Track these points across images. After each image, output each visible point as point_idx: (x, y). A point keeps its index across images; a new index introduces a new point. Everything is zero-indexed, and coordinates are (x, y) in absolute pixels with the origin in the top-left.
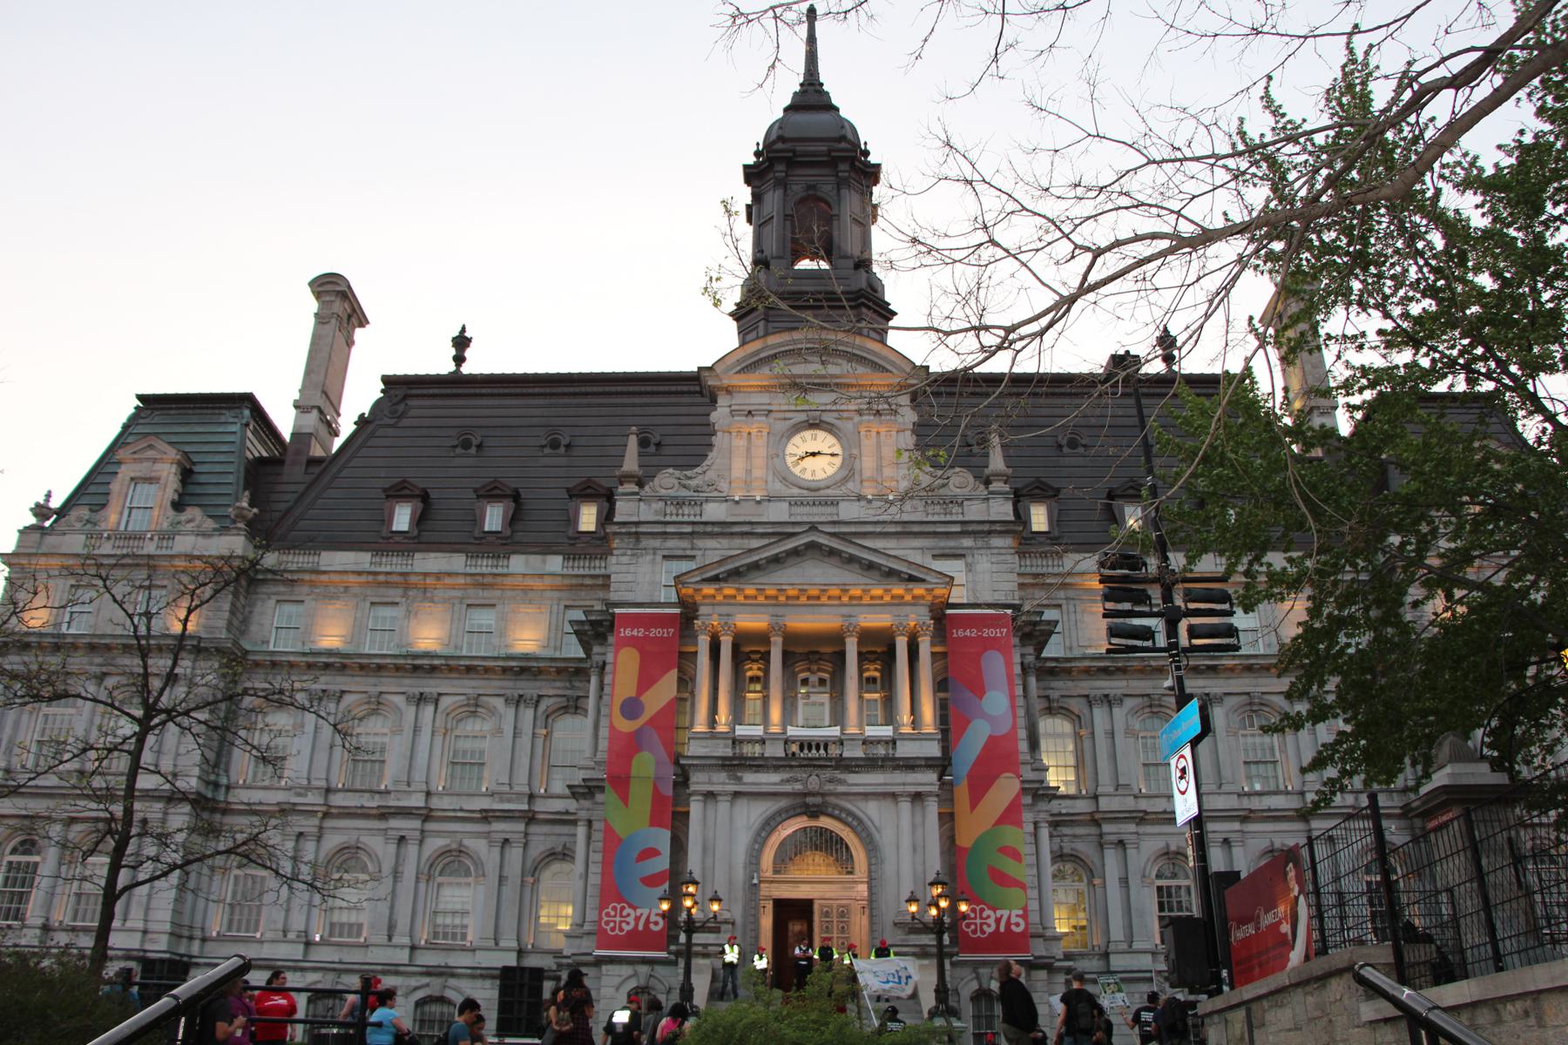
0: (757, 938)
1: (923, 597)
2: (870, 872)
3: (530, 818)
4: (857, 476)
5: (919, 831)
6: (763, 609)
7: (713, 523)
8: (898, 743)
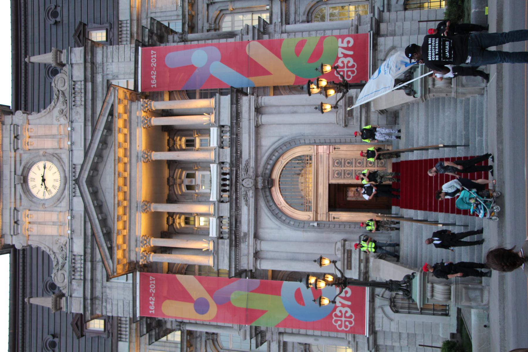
0: (355, 223)
1: (125, 106)
2: (310, 144)
4: (58, 151)
5: (281, 109)
6: (133, 217)
7: (85, 248)
8: (222, 123)
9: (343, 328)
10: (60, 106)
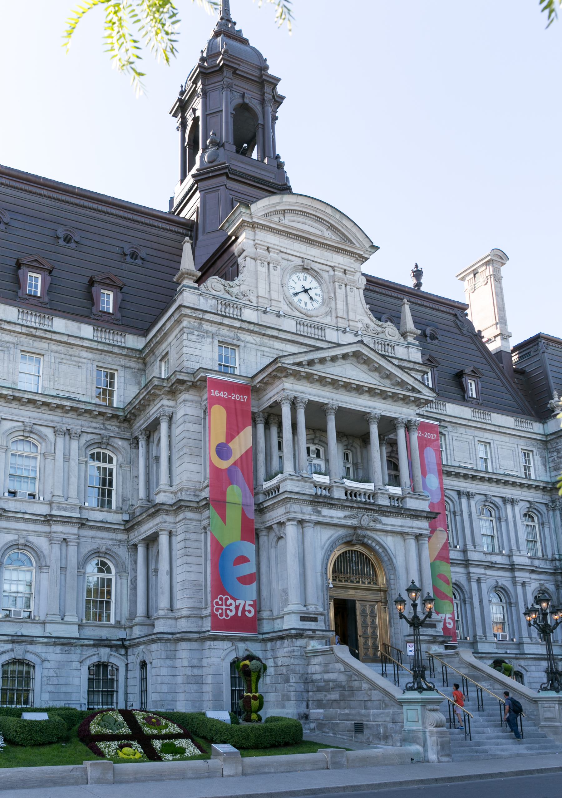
3: (82, 523)
9: (216, 606)
10: (372, 325)
